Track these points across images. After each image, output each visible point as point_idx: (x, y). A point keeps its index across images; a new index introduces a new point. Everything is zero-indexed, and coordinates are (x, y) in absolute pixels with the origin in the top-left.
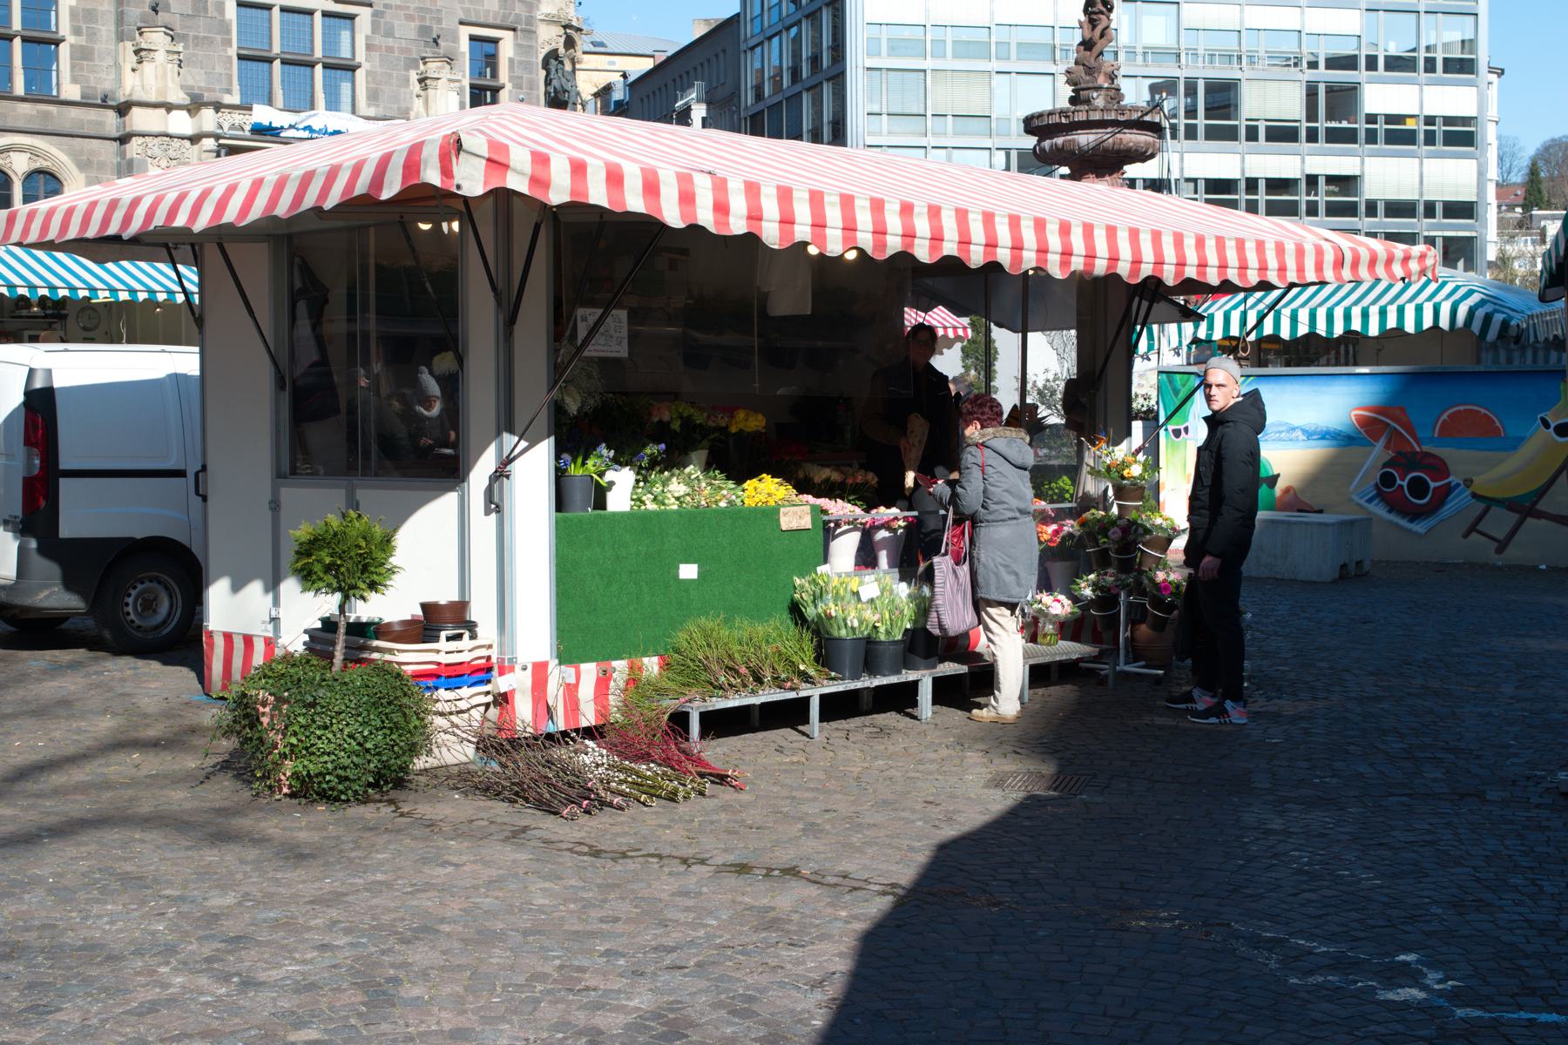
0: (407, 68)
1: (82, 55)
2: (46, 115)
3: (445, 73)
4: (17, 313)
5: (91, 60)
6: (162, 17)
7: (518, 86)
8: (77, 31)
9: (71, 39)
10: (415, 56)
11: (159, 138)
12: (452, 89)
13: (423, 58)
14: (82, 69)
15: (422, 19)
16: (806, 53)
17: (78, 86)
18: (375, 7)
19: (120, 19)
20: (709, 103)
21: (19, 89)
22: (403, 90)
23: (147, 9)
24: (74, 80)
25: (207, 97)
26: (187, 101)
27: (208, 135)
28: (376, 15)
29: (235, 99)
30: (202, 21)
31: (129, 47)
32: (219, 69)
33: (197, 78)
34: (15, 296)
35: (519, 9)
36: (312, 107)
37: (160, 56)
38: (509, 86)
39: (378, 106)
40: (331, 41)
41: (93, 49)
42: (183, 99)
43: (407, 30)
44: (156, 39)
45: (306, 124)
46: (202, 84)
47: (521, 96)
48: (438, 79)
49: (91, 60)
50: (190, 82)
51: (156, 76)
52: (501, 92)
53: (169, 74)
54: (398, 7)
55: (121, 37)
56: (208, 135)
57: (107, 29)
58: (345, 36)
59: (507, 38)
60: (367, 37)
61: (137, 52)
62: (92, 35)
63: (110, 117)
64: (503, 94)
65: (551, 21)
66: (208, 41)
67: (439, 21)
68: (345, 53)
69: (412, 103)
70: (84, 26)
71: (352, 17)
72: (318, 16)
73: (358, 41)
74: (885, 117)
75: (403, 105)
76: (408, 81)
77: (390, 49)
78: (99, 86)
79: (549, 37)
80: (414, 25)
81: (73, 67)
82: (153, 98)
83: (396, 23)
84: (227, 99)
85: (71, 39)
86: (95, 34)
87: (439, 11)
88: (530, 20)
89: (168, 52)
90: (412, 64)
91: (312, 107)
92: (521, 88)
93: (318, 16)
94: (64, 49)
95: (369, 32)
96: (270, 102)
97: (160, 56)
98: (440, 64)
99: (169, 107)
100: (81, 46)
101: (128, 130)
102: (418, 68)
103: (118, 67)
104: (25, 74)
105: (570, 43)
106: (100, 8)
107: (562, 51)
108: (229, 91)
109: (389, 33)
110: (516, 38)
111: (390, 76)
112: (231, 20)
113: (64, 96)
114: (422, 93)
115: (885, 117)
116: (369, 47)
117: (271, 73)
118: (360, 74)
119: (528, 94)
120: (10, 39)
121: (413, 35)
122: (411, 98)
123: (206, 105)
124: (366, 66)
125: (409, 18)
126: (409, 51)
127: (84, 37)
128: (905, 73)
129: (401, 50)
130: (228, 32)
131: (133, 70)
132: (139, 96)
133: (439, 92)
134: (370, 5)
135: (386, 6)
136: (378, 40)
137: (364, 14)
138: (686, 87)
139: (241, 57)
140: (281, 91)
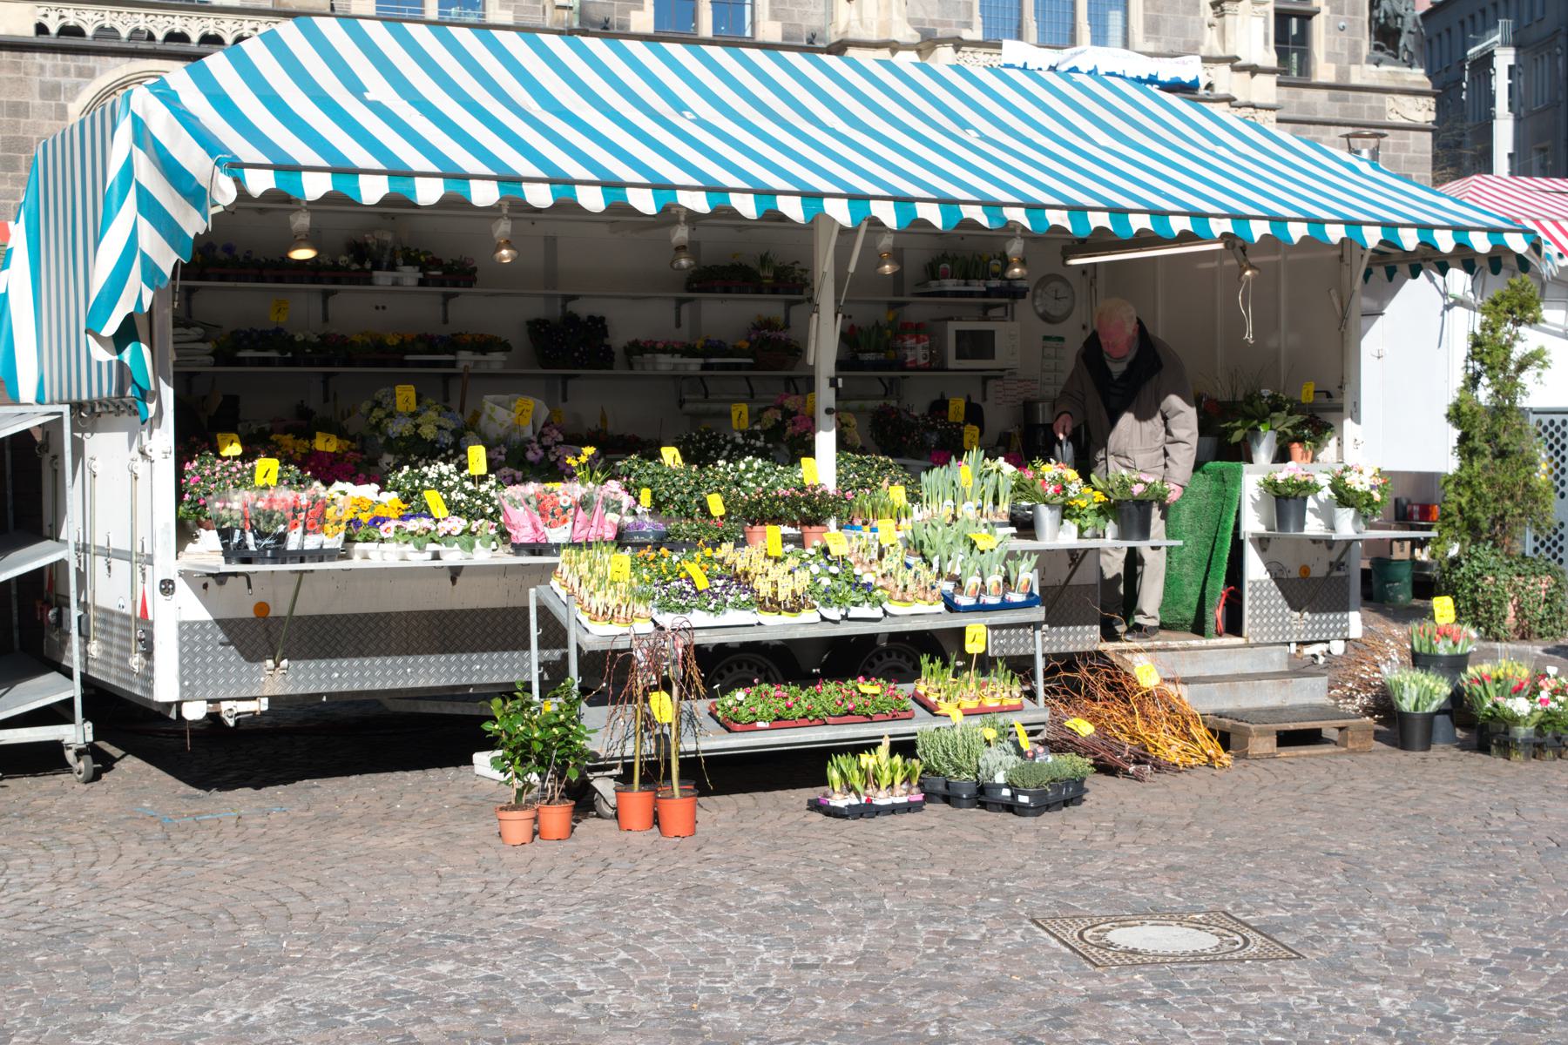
4: (934, 286)
7: (1338, 10)
12: (1256, 15)
17: (779, 24)
20: (1518, 46)
21: (706, 28)
22: (1191, 18)
24: (774, 16)
25: (941, 32)
26: (917, 38)
29: (976, 34)
34: (1042, 230)
36: (1073, 42)
38: (1325, 10)
39: (1158, 40)
42: (912, 36)
46: (935, 17)
47: (1342, 24)
50: (920, 15)
51: (879, 8)
52: (1315, 19)
64: (1318, 26)
75: (1191, 38)
76: (1198, 6)
78: (804, 24)
82: (874, 36)
84: (967, 35)
91: (1073, 42)
92: (1341, 12)
96: (1019, 37)
99: (894, 46)
104: (713, 10)
108: (968, 25)
113: (762, 37)
114: (1216, 21)
119: (1351, 20)
122: (1202, 28)
123: (943, 41)
132: (856, 33)
133: (1239, 18)
138: (1488, 26)
140: (1035, 24)
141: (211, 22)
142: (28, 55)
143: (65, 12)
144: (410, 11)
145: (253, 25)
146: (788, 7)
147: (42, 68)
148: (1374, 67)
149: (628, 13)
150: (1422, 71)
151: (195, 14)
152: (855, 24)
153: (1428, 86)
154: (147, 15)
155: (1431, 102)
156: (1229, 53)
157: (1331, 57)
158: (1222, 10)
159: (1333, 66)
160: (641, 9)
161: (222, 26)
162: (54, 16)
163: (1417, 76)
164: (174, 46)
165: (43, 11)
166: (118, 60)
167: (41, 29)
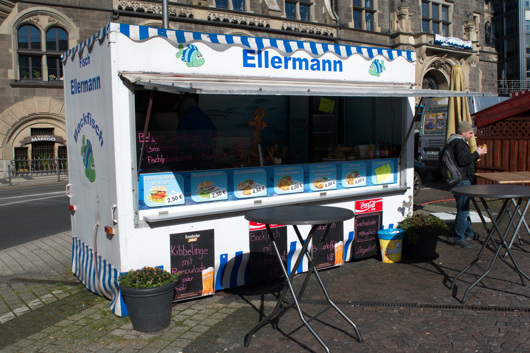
0: (462, 25)
1: (381, 16)
2: (372, 38)
3: (474, 27)
5: (383, 19)
8: (379, 9)
9: (378, 11)
10: (463, 21)
11: (407, 46)
13: (466, 21)
18: (455, 4)
22: (461, 32)
24: (379, 26)
27: (424, 44)
28: (455, 6)
32: (418, 23)
37: (407, 17)
41: (384, 15)
43: (461, 12)
45: (448, 41)
48: (472, 28)
49: (383, 19)
51: (406, 24)
54: (460, 4)
55: (392, 10)
56: (424, 44)
57: (387, 8)
59: (478, 15)
60: (453, 13)
62: (383, 10)
63: (388, 39)
69: (463, 37)
72: (440, 6)
77: (458, 18)
80: (463, 10)
81: (379, 21)
83: (459, 9)
85: (378, 11)
87: (469, 6)
89: (410, 16)
90: (463, 24)
93: (440, 6)
95: (453, 12)
97: (407, 17)
98: (473, 23)
100: (381, 14)
101: (396, 43)
102: (464, 25)
103: (391, 22)
109: (458, 13)
114: (466, 33)
116: (453, 17)
118: (451, 26)
121: (463, 13)
124: (452, 23)
125: (462, 8)
130: (420, 10)
131: (397, 22)
133: (472, 32)
134: (453, 2)
135: (457, 3)
136: (455, 15)
137: (452, 5)
139: (423, 20)
141: (252, 19)
142: (206, 26)
143: (215, 14)
145: (262, 20)
146: (382, 23)
147: (210, 30)
148: (486, 47)
149: (348, 23)
150: (494, 49)
151: (248, 16)
152: (400, 28)
153: (496, 52)
154: (236, 16)
155: (496, 56)
160: (351, 22)
162: (212, 14)
163: (493, 50)
164: (243, 25)
165: (209, 13)
166: (229, 29)
167: (209, 19)
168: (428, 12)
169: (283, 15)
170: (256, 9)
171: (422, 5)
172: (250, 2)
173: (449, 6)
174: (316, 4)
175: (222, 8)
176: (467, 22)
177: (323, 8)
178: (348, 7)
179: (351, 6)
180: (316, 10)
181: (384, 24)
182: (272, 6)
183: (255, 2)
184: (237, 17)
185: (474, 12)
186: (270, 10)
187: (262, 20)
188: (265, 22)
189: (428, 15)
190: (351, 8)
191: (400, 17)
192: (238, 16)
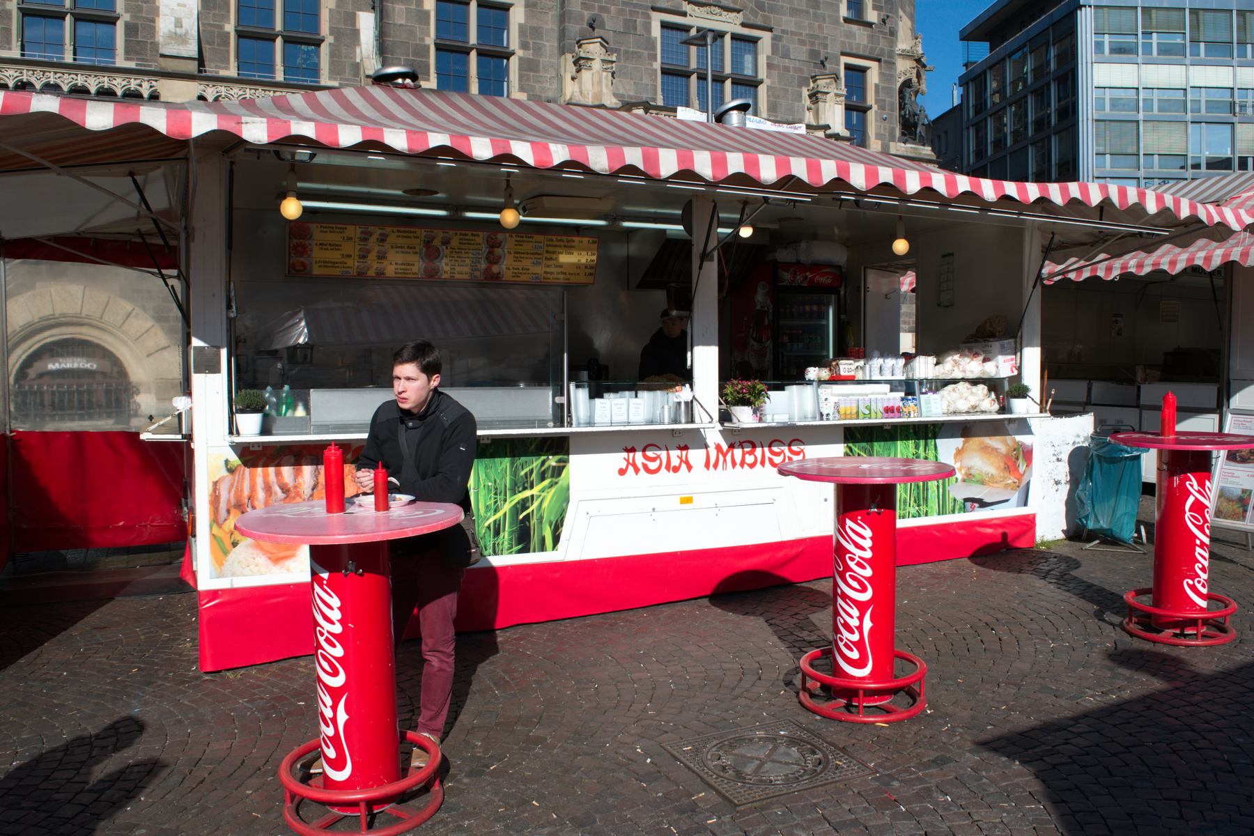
0: (800, 86)
1: (528, 66)
3: (833, 90)
5: (538, 71)
6: (597, 32)
7: (881, 108)
8: (524, 46)
9: (520, 53)
10: (806, 75)
12: (837, 103)
14: (528, 79)
15: (813, 44)
16: (990, 138)
17: (525, 94)
18: (775, 32)
19: (562, 34)
22: (796, 104)
23: (585, 26)
24: (522, 89)
28: (774, 38)
30: (631, 38)
31: (569, 58)
33: (630, 91)
35: (883, 44)
37: (597, 65)
40: (737, 62)
41: (539, 62)
42: (616, 104)
43: (800, 53)
44: (593, 49)
46: (632, 93)
47: (885, 116)
48: (827, 93)
50: (621, 91)
51: (593, 84)
52: (869, 113)
53: (604, 81)
54: (793, 33)
57: (550, 45)
58: (748, 59)
60: (768, 57)
61: (575, 63)
62: (538, 50)
65: (906, 55)
66: (638, 56)
67: (825, 46)
68: (748, 71)
69: (804, 115)
70: (531, 42)
71: (754, 41)
73: (761, 62)
74: (1108, 157)
76: (801, 96)
77: (787, 69)
79: (904, 68)
81: (521, 77)
86: (540, 48)
88: (891, 54)
90: (803, 83)
92: (884, 109)
93: (728, 38)
94: (514, 63)
95: (770, 54)
96: (687, 105)
97: (597, 65)
98: (828, 81)
102: (809, 85)
103: (560, 78)
104: (479, 83)
105: (919, 76)
106: (545, 26)
107: (915, 80)
109: (786, 55)
110: (880, 67)
111: (787, 91)
112: (656, 38)
114: (813, 107)
115: (1108, 157)
116: (770, 66)
117: (688, 86)
118: (762, 90)
119: (890, 114)
120: (467, 52)
121: (804, 57)
122: (803, 111)
124: (767, 82)
125: (802, 43)
126: (801, 70)
127: (531, 51)
128: (1124, 124)
129: (796, 70)
130: (654, 48)
131: (573, 79)
133: (827, 104)
134: (770, 30)
135: (783, 31)
137: (766, 38)
139: (665, 72)
140: (697, 102)
141: (106, 79)
144: (259, 76)
145: (138, 82)
146: (532, 83)
148: (903, 145)
150: (930, 148)
151: (93, 74)
152: (577, 94)
154: (56, 73)
156: (822, 122)
157: (878, 136)
158: (817, 99)
159: (880, 142)
161: (114, 82)
168: (722, 60)
169: (227, 68)
170: (143, 57)
171: (662, 36)
172: (126, 41)
173: (759, 39)
174: (336, 39)
175: (40, 56)
176: (814, 79)
177: (358, 51)
178: (417, 45)
179: (430, 40)
180: (333, 54)
181: (537, 86)
182: (176, 47)
183: (140, 39)
184: (58, 75)
185: (843, 54)
186: (163, 56)
187: (138, 82)
188: (146, 85)
189: (688, 61)
190: (428, 47)
191: (579, 63)
192: (63, 74)
